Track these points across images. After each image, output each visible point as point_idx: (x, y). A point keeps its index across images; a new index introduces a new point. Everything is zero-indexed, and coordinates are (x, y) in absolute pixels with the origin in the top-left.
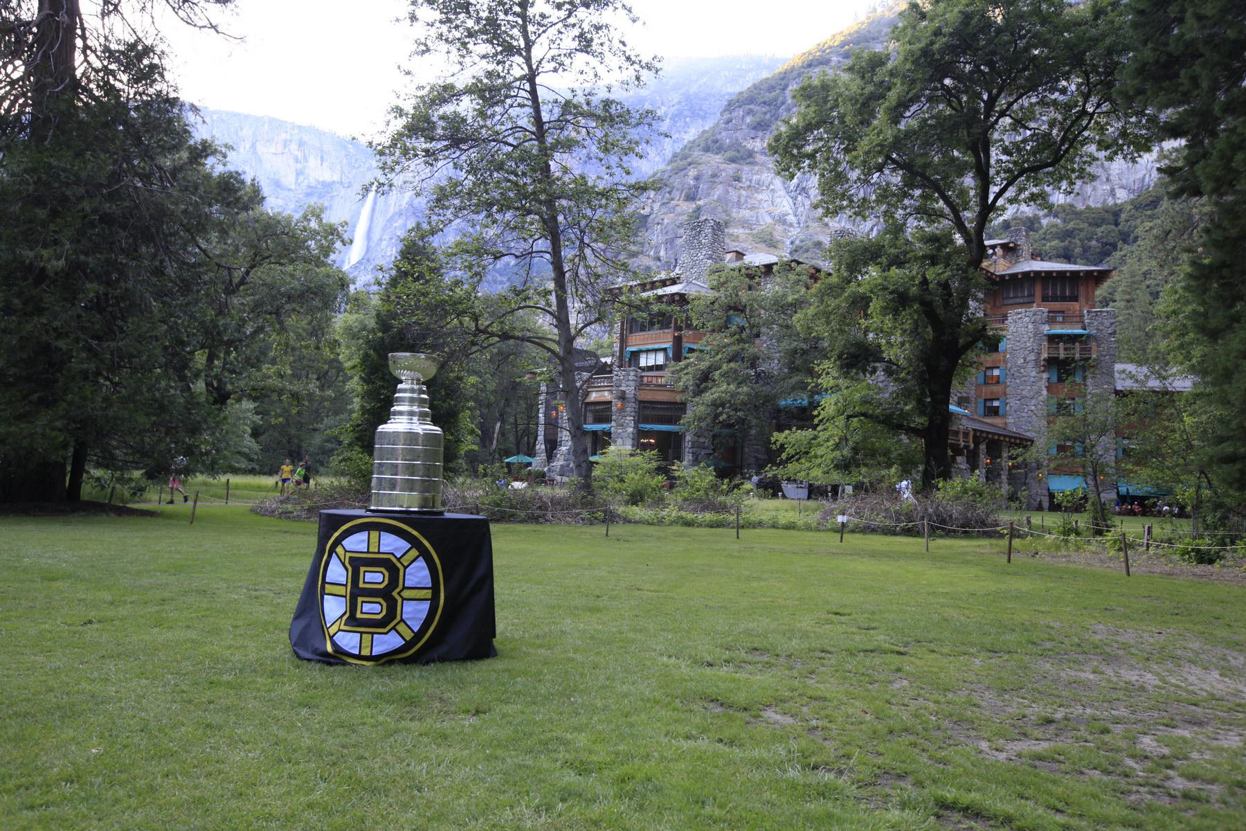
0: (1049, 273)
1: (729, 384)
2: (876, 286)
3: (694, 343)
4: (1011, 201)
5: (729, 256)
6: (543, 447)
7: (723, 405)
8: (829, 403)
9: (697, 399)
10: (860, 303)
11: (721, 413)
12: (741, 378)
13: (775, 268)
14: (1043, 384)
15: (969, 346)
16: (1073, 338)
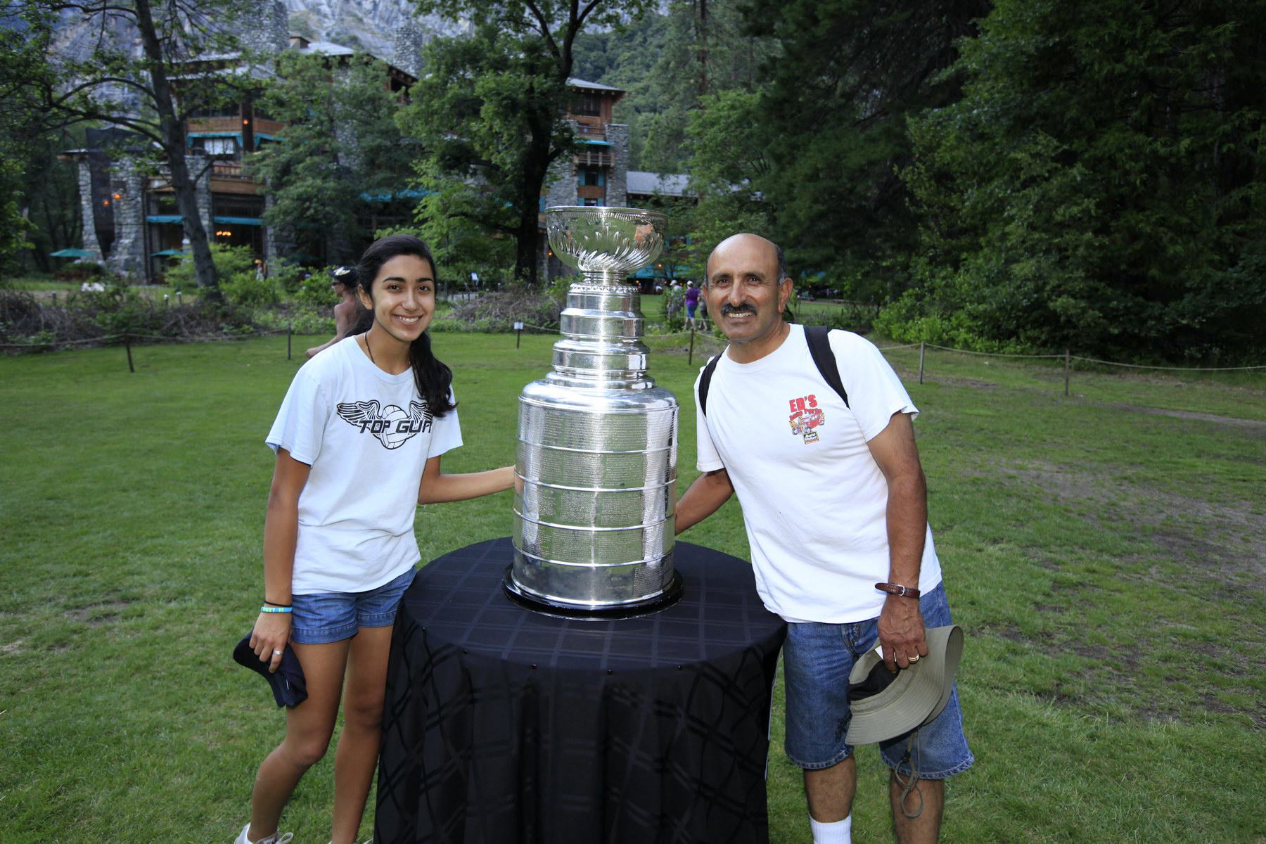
0: (578, 89)
1: (314, 178)
2: (491, 90)
3: (266, 133)
4: (593, 20)
5: (293, 42)
6: (93, 237)
7: (309, 199)
8: (431, 203)
9: (281, 193)
10: (468, 108)
11: (308, 208)
12: (325, 173)
13: (351, 61)
14: (575, 186)
15: (557, 153)
16: (596, 148)
